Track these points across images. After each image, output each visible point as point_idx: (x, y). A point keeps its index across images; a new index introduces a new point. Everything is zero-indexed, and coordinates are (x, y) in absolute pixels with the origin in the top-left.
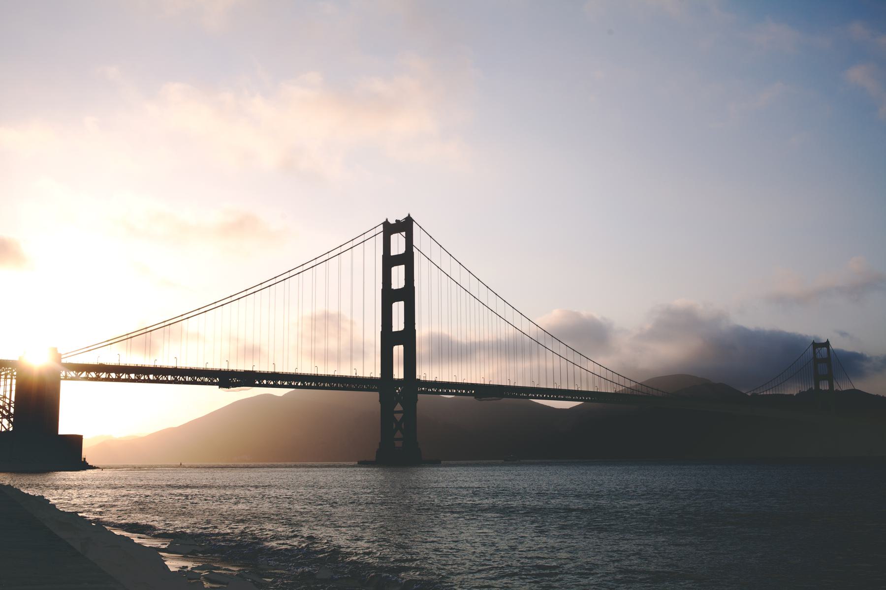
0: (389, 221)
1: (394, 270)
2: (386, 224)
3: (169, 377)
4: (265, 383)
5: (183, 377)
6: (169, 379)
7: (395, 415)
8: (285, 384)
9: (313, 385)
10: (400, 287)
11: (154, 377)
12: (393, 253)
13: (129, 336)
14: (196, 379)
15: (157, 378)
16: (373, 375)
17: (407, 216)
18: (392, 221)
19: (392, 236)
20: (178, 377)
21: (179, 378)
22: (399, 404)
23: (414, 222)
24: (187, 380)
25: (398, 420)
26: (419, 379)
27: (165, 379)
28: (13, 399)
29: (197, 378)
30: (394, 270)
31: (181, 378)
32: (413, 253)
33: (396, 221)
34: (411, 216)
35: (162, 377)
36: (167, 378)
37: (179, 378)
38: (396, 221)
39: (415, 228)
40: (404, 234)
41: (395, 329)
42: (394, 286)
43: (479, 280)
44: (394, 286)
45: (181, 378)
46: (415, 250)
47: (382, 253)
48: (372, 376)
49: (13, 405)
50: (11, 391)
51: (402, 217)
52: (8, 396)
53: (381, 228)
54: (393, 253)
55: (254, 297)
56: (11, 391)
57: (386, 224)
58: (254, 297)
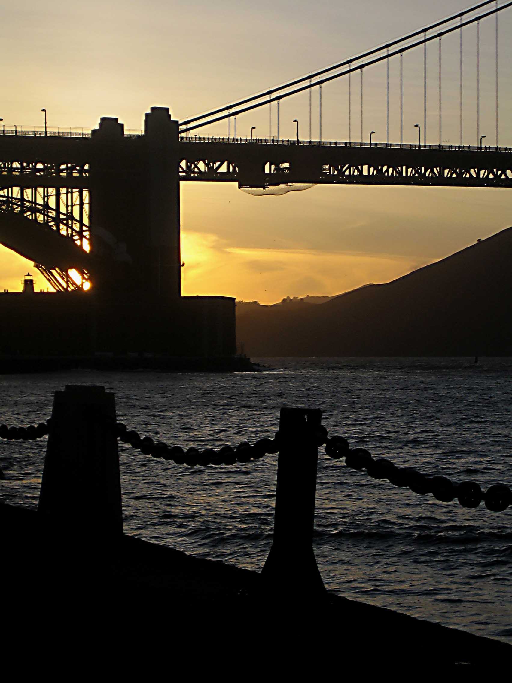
3: (365, 167)
5: (394, 169)
6: (365, 173)
11: (332, 169)
13: (315, 80)
14: (423, 172)
15: (340, 172)
20: (385, 168)
21: (387, 171)
24: (404, 174)
27: (356, 173)
28: (86, 221)
29: (426, 171)
31: (391, 170)
35: (349, 168)
36: (361, 172)
37: (387, 171)
45: (391, 170)
49: (86, 234)
50: (81, 204)
52: (76, 215)
56: (81, 204)
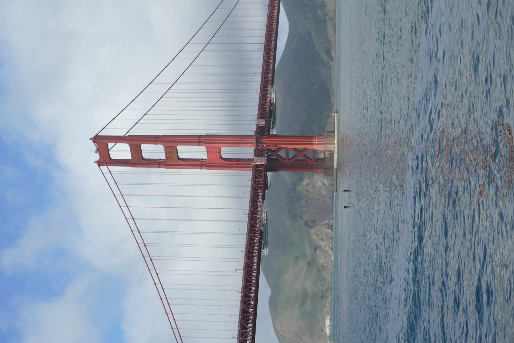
0: (96, 160)
1: (145, 156)
2: (100, 163)
4: (252, 310)
7: (290, 157)
8: (254, 289)
9: (255, 261)
10: (163, 149)
12: (128, 156)
16: (250, 178)
17: (91, 141)
18: (97, 157)
19: (112, 158)
22: (278, 153)
23: (98, 135)
25: (295, 154)
26: (255, 131)
30: (145, 156)
32: (129, 136)
33: (96, 152)
34: (92, 136)
38: (96, 152)
39: (103, 134)
40: (110, 145)
41: (205, 156)
42: (162, 156)
43: (158, 75)
44: (162, 156)
46: (127, 135)
47: (130, 167)
48: (251, 179)
51: (93, 147)
53: (104, 168)
54: (128, 156)
55: (169, 298)
57: (100, 163)
58: (169, 298)
